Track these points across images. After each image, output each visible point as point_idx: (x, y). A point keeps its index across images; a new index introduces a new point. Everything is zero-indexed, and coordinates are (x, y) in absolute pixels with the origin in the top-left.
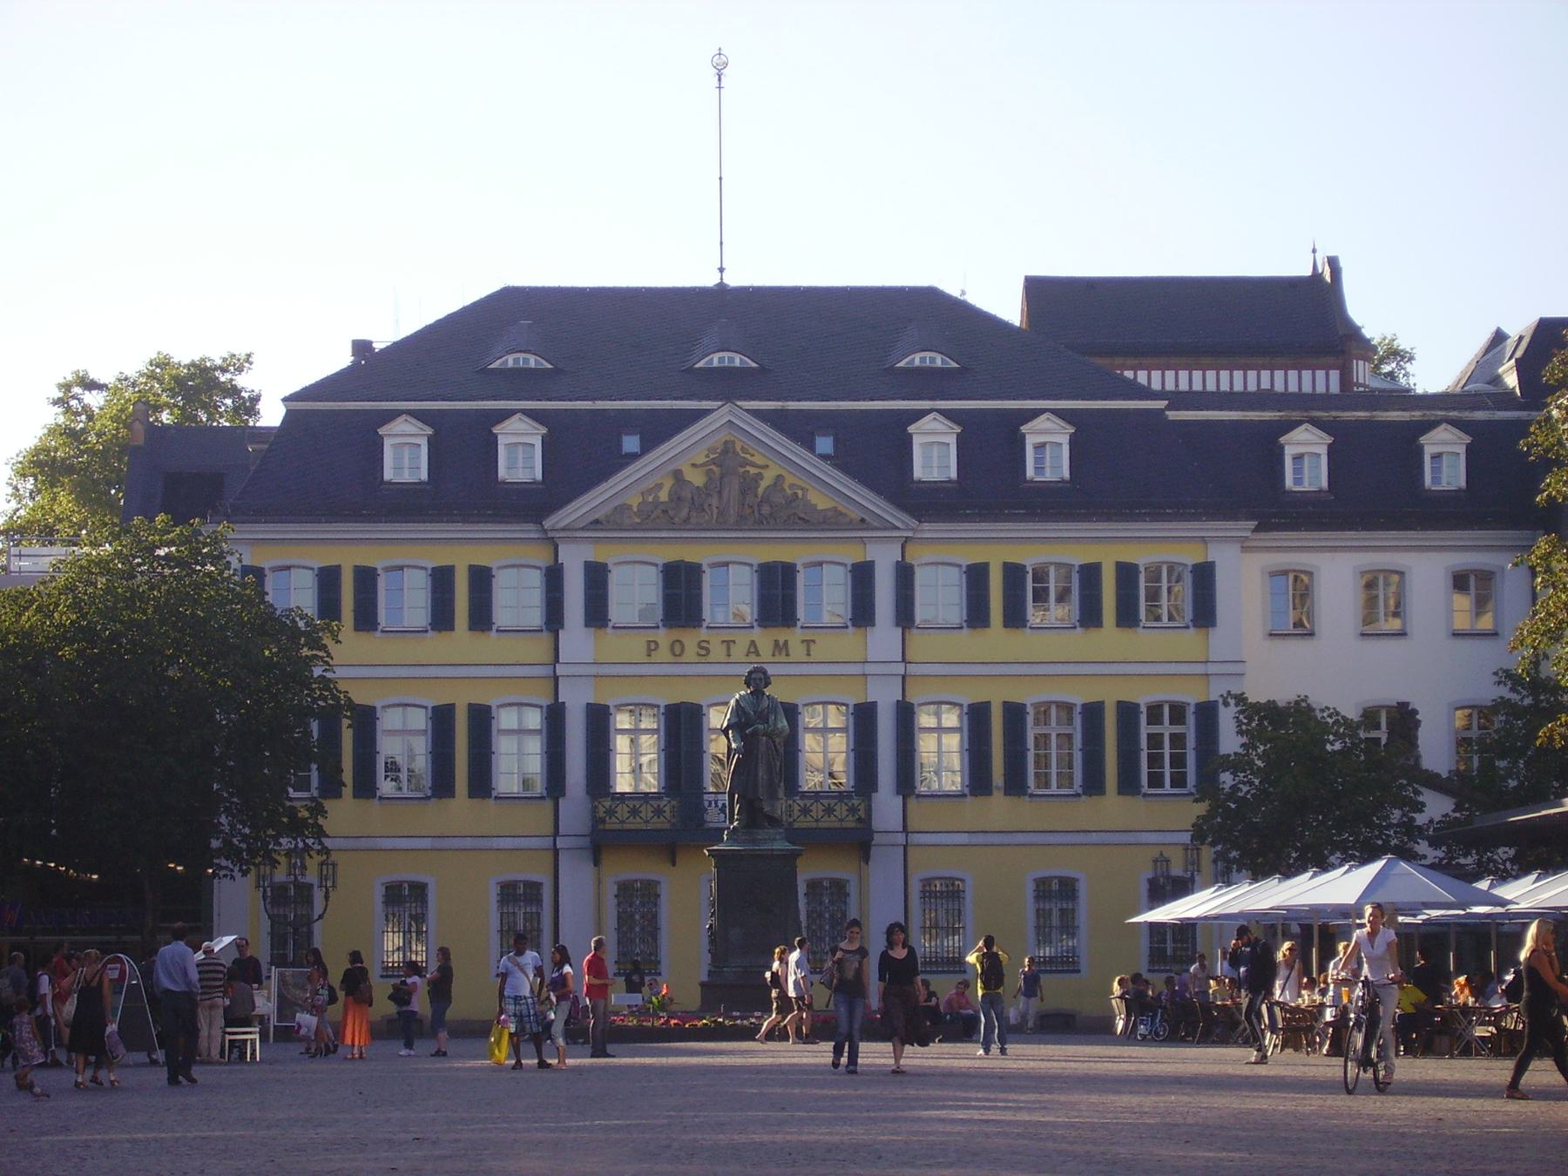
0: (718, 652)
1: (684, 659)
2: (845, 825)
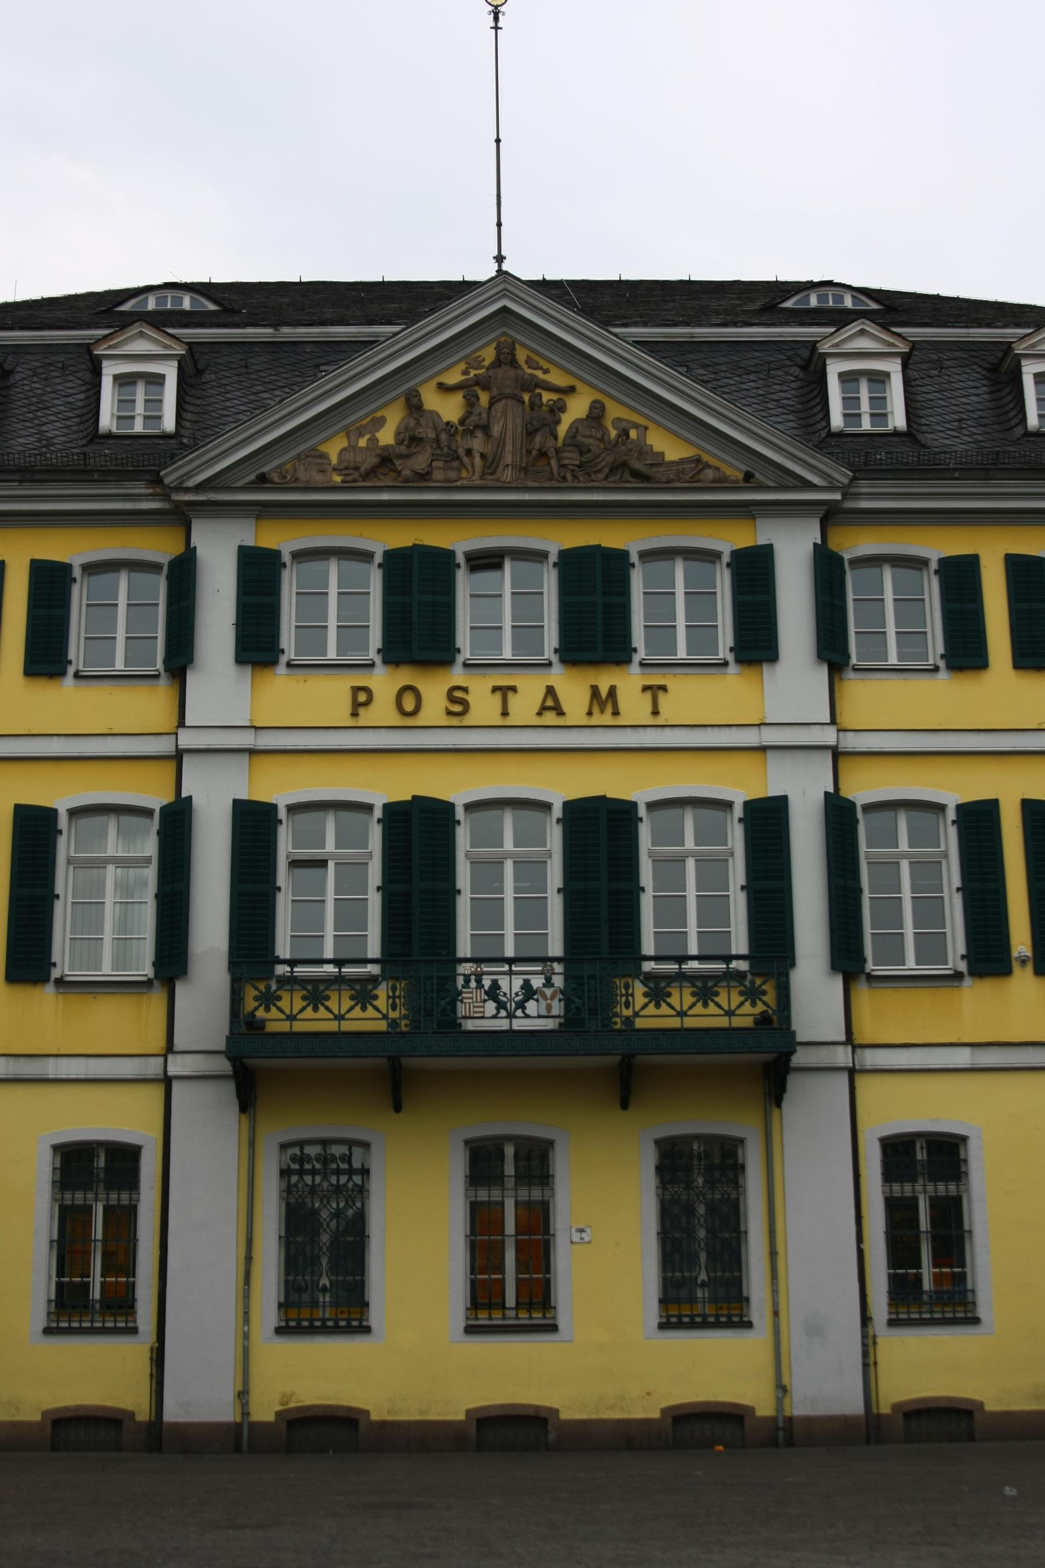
0: (483, 705)
1: (420, 720)
2: (737, 1022)
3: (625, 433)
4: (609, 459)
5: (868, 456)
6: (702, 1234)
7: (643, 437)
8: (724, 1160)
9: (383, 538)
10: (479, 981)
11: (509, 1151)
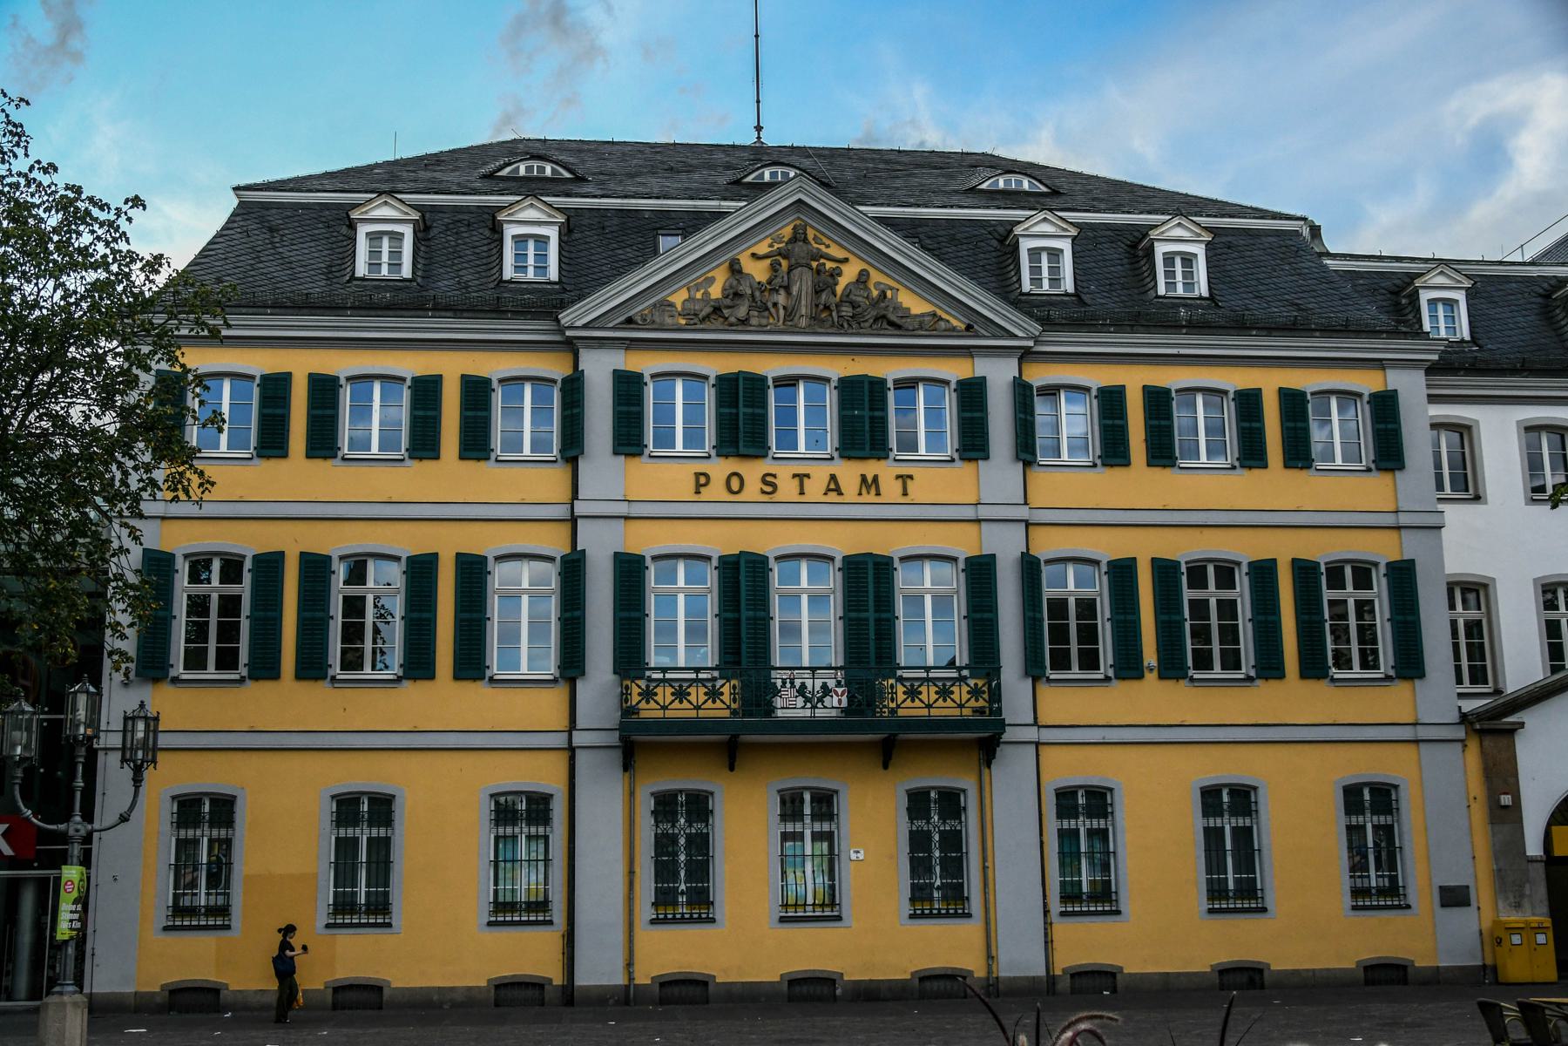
0: (787, 488)
2: (966, 712)
3: (883, 295)
4: (874, 313)
5: (1052, 314)
6: (937, 854)
7: (895, 296)
8: (951, 802)
9: (714, 365)
10: (792, 683)
11: (807, 797)
